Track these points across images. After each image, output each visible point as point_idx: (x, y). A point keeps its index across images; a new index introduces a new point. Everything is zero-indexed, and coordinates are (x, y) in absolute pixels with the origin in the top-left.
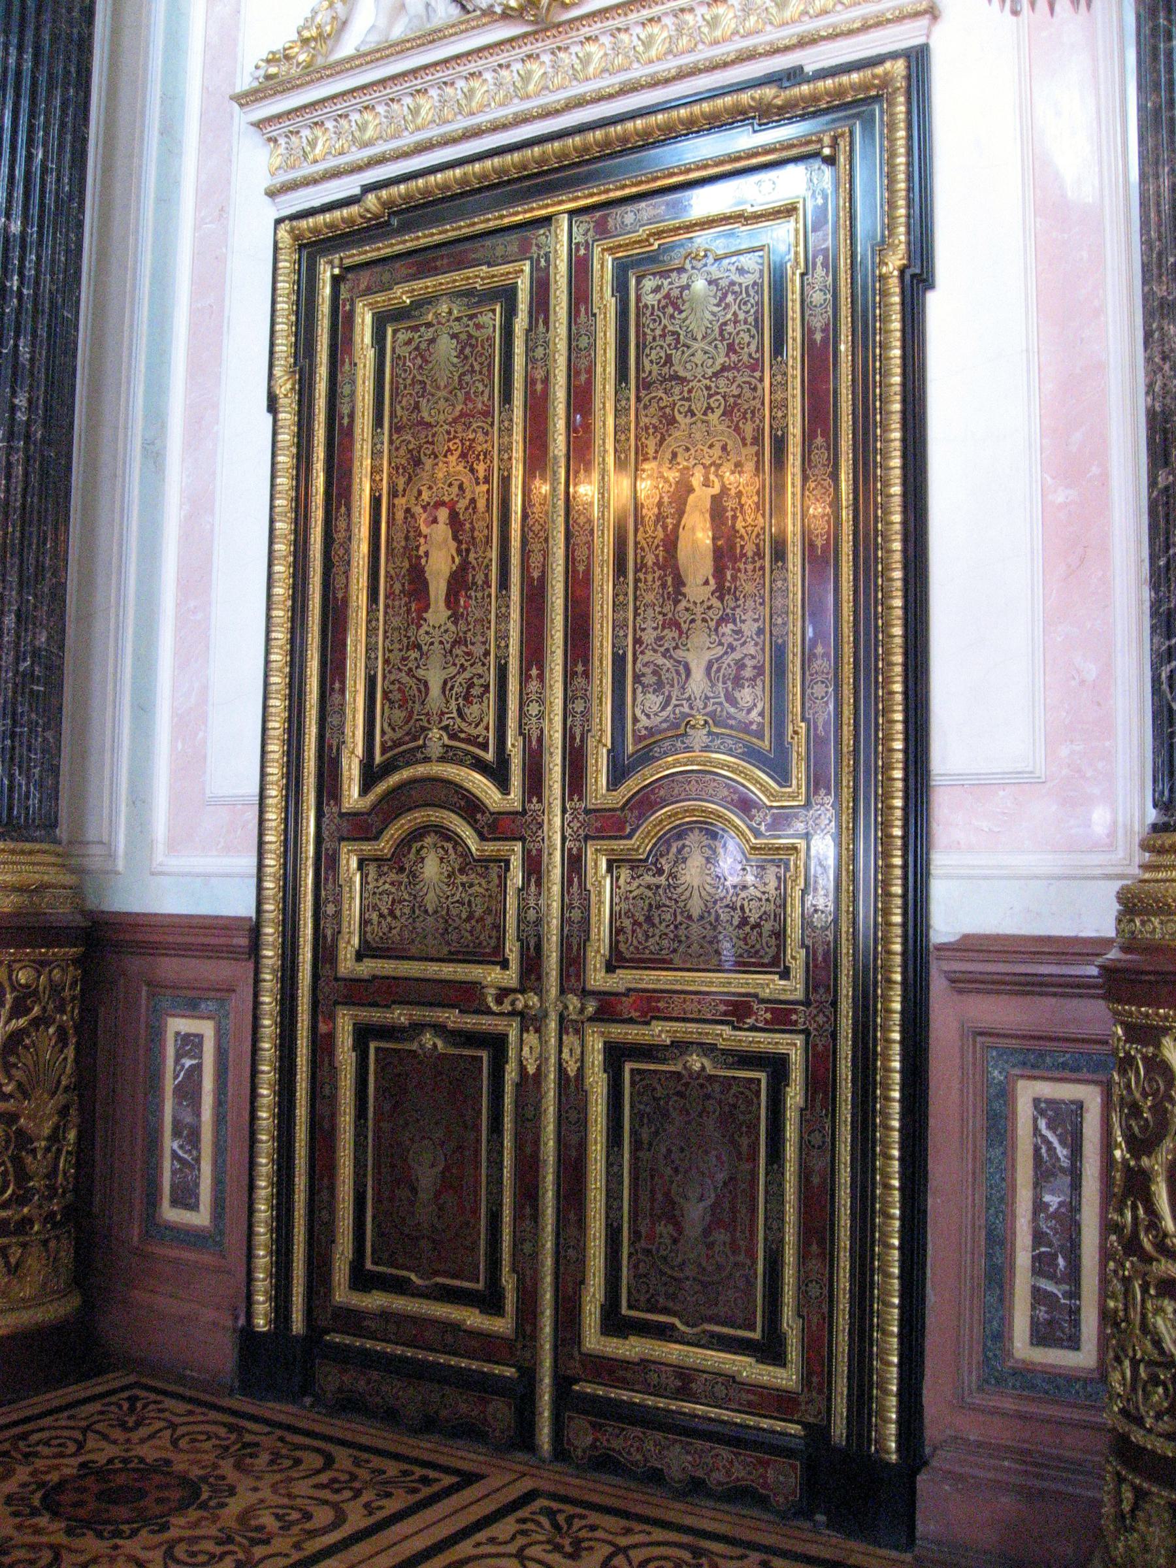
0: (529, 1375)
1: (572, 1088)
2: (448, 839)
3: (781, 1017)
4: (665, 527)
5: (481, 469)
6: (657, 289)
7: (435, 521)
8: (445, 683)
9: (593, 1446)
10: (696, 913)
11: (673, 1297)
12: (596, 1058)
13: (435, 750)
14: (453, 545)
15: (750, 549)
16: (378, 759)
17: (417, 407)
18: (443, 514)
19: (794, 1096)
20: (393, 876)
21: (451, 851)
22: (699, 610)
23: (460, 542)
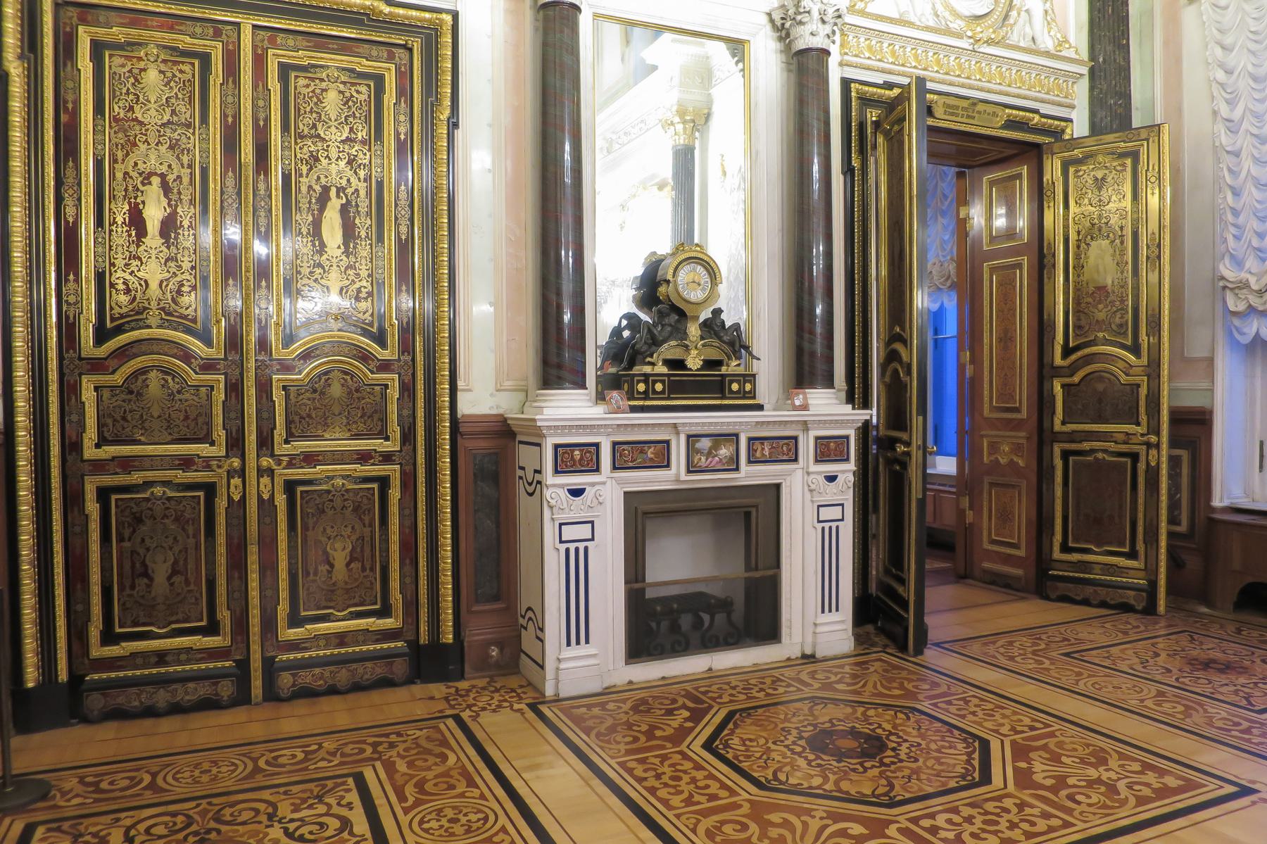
0: (244, 665)
1: (266, 506)
2: (168, 374)
3: (387, 458)
4: (313, 215)
5: (185, 159)
6: (307, 86)
7: (150, 183)
8: (161, 282)
9: (294, 685)
10: (156, 415)
11: (331, 600)
12: (279, 487)
13: (153, 321)
14: (164, 202)
15: (363, 234)
16: (109, 325)
17: (131, 109)
18: (156, 181)
19: (395, 494)
20: (123, 396)
21: (170, 380)
22: (334, 260)
23: (170, 200)
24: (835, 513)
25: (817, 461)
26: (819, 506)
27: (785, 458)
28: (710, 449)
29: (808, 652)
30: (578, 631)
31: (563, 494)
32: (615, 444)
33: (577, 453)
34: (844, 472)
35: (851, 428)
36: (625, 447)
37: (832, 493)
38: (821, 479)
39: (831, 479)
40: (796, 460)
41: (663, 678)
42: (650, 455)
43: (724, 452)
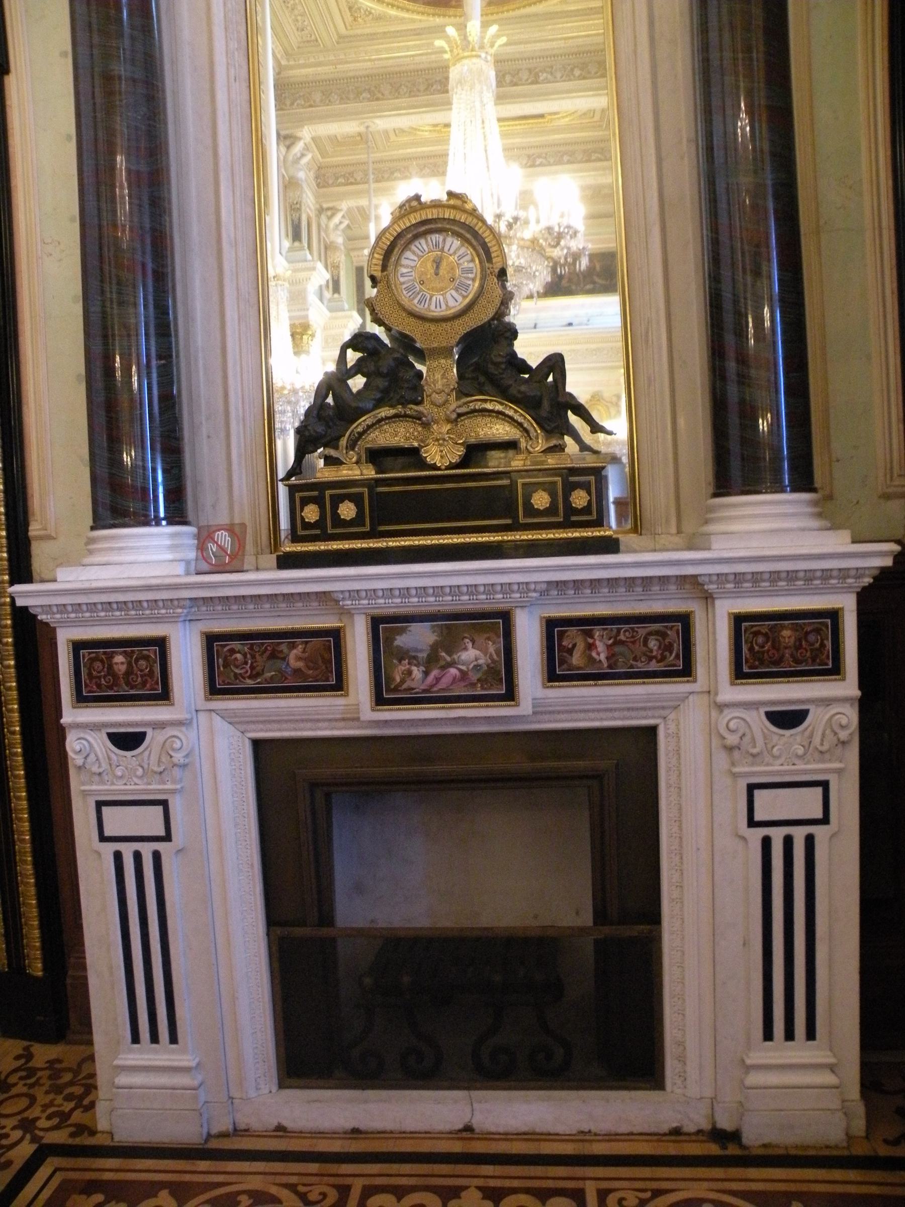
24: (808, 803)
25: (740, 674)
26: (751, 789)
27: (653, 666)
28: (434, 648)
29: (725, 1123)
30: (156, 1016)
31: (100, 743)
32: (211, 640)
33: (119, 659)
34: (827, 702)
35: (848, 589)
36: (236, 645)
37: (787, 753)
38: (758, 721)
39: (787, 718)
40: (686, 671)
41: (356, 1131)
42: (294, 663)
43: (470, 655)
